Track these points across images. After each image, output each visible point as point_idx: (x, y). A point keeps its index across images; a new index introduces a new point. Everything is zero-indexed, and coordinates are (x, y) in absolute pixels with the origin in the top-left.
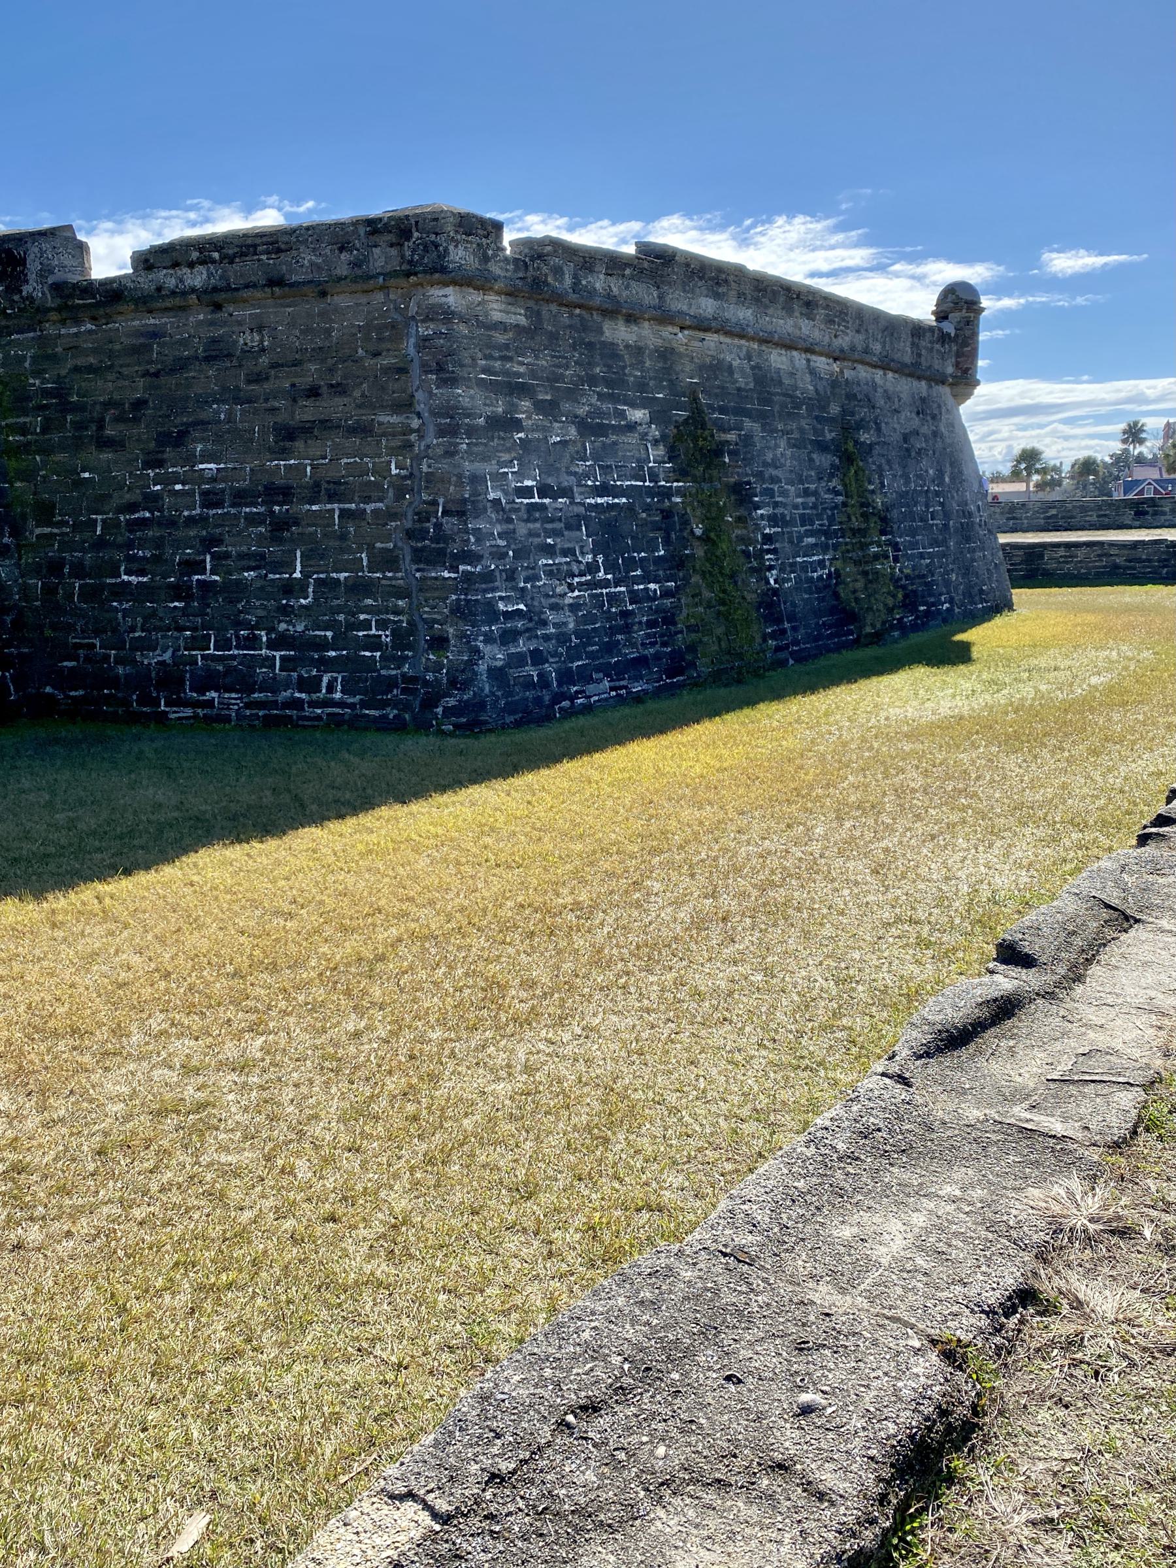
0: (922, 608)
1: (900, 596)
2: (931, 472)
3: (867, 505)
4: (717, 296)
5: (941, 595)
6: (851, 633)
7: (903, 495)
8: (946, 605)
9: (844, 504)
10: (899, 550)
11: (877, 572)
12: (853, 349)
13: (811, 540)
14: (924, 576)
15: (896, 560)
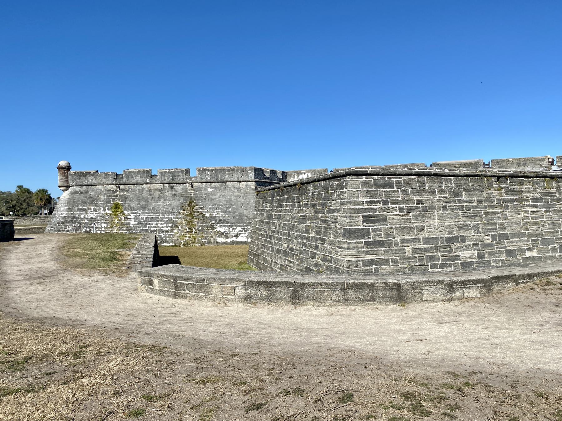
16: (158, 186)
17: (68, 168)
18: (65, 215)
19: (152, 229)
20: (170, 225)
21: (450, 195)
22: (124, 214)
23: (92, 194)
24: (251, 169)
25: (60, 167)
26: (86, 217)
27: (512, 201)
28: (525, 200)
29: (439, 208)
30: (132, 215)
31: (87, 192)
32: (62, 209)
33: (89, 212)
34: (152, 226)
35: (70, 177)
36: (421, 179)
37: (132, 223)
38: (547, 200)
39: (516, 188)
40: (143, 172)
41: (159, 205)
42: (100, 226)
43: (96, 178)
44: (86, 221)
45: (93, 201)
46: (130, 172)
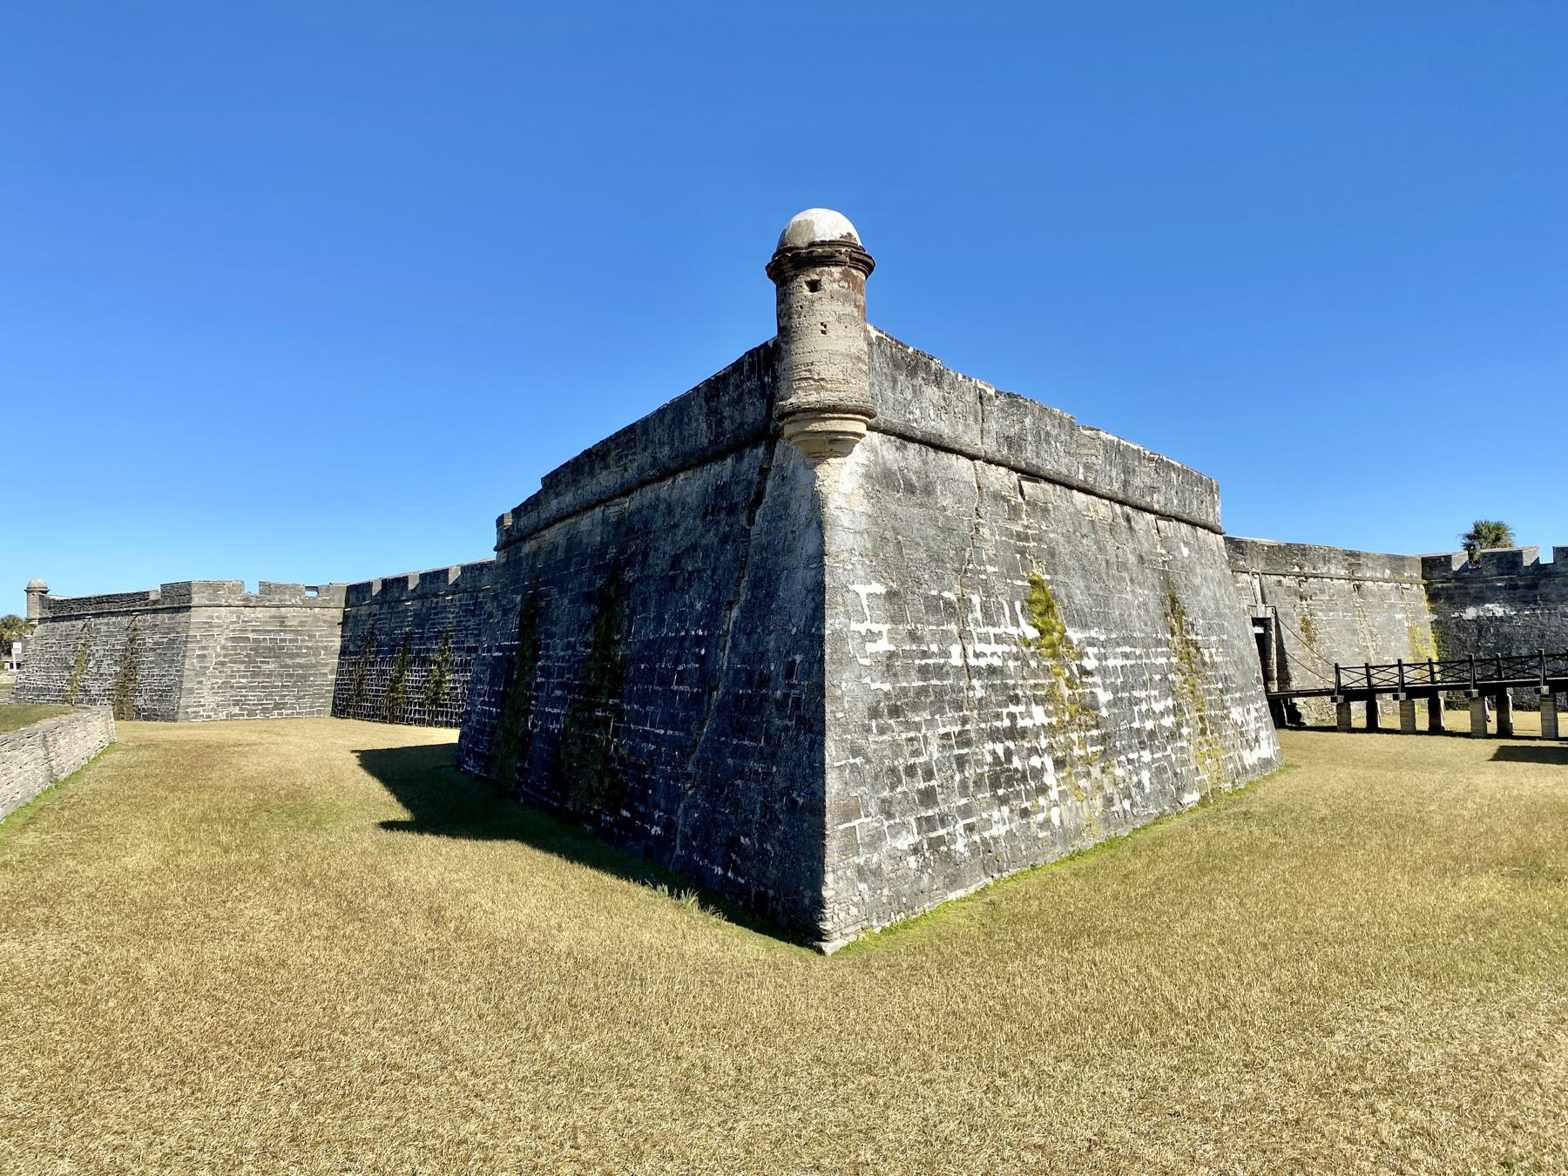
0: (625, 813)
1: (607, 782)
2: (699, 606)
3: (608, 658)
4: (557, 495)
5: (657, 806)
6: (555, 798)
7: (648, 645)
8: (656, 830)
9: (590, 657)
10: (621, 720)
11: (593, 740)
12: (641, 470)
13: (558, 693)
14: (642, 769)
15: (616, 733)
16: (1103, 509)
18: (883, 646)
19: (1149, 725)
20: (1170, 702)
22: (1069, 641)
26: (972, 661)
30: (1091, 651)
31: (928, 490)
32: (862, 590)
33: (972, 627)
34: (1144, 707)
37: (1104, 697)
41: (1129, 605)
42: (1027, 723)
43: (945, 408)
46: (1043, 410)
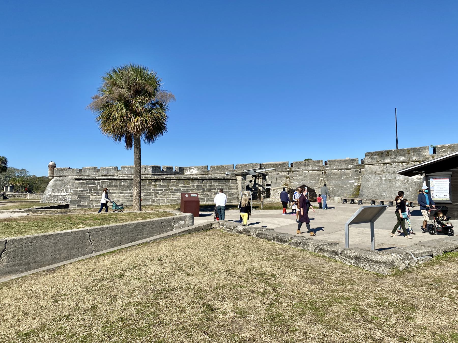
17: (54, 166)
21: (125, 188)
23: (65, 181)
24: (150, 167)
25: (49, 166)
27: (162, 190)
28: (170, 190)
29: (118, 193)
31: (63, 180)
35: (54, 171)
36: (110, 181)
38: (183, 189)
39: (166, 184)
40: (92, 169)
44: (61, 197)
45: (65, 185)
46: (85, 169)
